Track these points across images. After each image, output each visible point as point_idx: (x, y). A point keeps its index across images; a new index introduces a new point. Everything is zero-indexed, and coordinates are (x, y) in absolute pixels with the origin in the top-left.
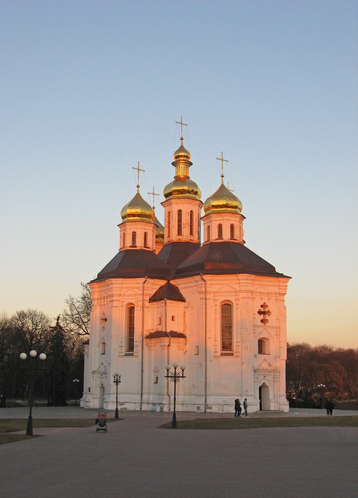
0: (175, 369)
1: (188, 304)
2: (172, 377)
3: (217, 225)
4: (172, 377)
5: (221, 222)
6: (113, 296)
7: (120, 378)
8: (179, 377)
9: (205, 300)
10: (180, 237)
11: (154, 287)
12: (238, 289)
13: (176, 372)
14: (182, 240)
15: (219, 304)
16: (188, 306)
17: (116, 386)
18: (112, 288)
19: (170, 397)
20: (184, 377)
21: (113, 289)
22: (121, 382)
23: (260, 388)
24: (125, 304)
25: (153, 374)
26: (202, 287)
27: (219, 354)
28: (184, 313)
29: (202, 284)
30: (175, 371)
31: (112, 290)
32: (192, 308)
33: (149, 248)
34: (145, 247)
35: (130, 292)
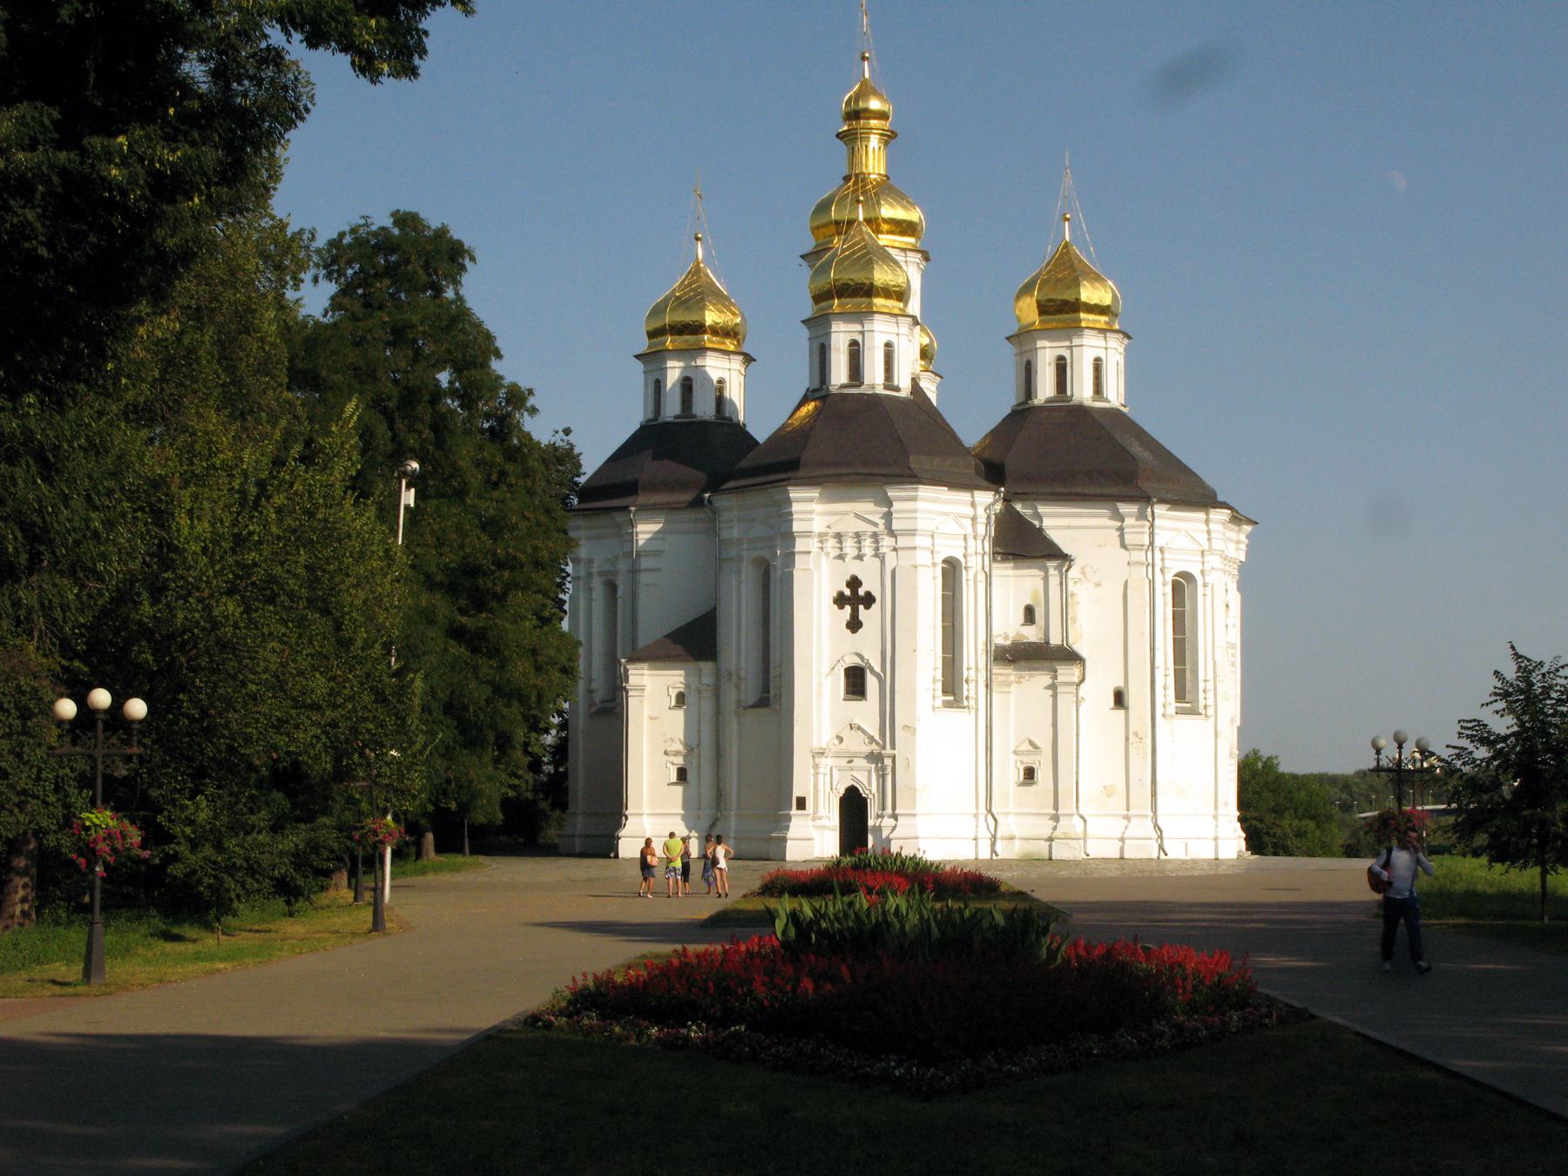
1: (1083, 573)
3: (1091, 361)
5: (1102, 354)
6: (914, 535)
9: (1145, 568)
12: (1206, 546)
15: (1169, 577)
16: (1082, 576)
18: (915, 511)
19: (1085, 821)
21: (918, 515)
24: (939, 559)
25: (1013, 757)
26: (1143, 533)
27: (1171, 710)
29: (1143, 526)
31: (916, 518)
32: (1098, 585)
35: (950, 526)
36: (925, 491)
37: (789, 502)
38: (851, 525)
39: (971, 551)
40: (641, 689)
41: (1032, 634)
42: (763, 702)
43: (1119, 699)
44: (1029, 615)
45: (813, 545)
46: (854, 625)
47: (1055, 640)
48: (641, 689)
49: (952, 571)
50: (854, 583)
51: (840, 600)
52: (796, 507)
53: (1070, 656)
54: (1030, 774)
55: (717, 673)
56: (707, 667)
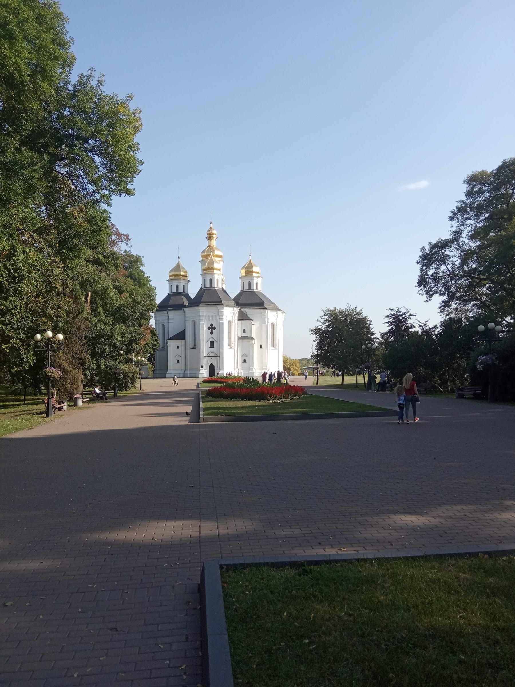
15: (270, 324)
36: (225, 308)
37: (199, 309)
38: (210, 314)
39: (233, 319)
40: (170, 345)
41: (244, 334)
42: (194, 348)
43: (261, 347)
44: (244, 331)
45: (204, 318)
46: (212, 333)
48: (170, 345)
49: (230, 322)
50: (212, 325)
51: (209, 328)
52: (200, 311)
53: (253, 339)
54: (245, 361)
55: (185, 342)
56: (183, 341)
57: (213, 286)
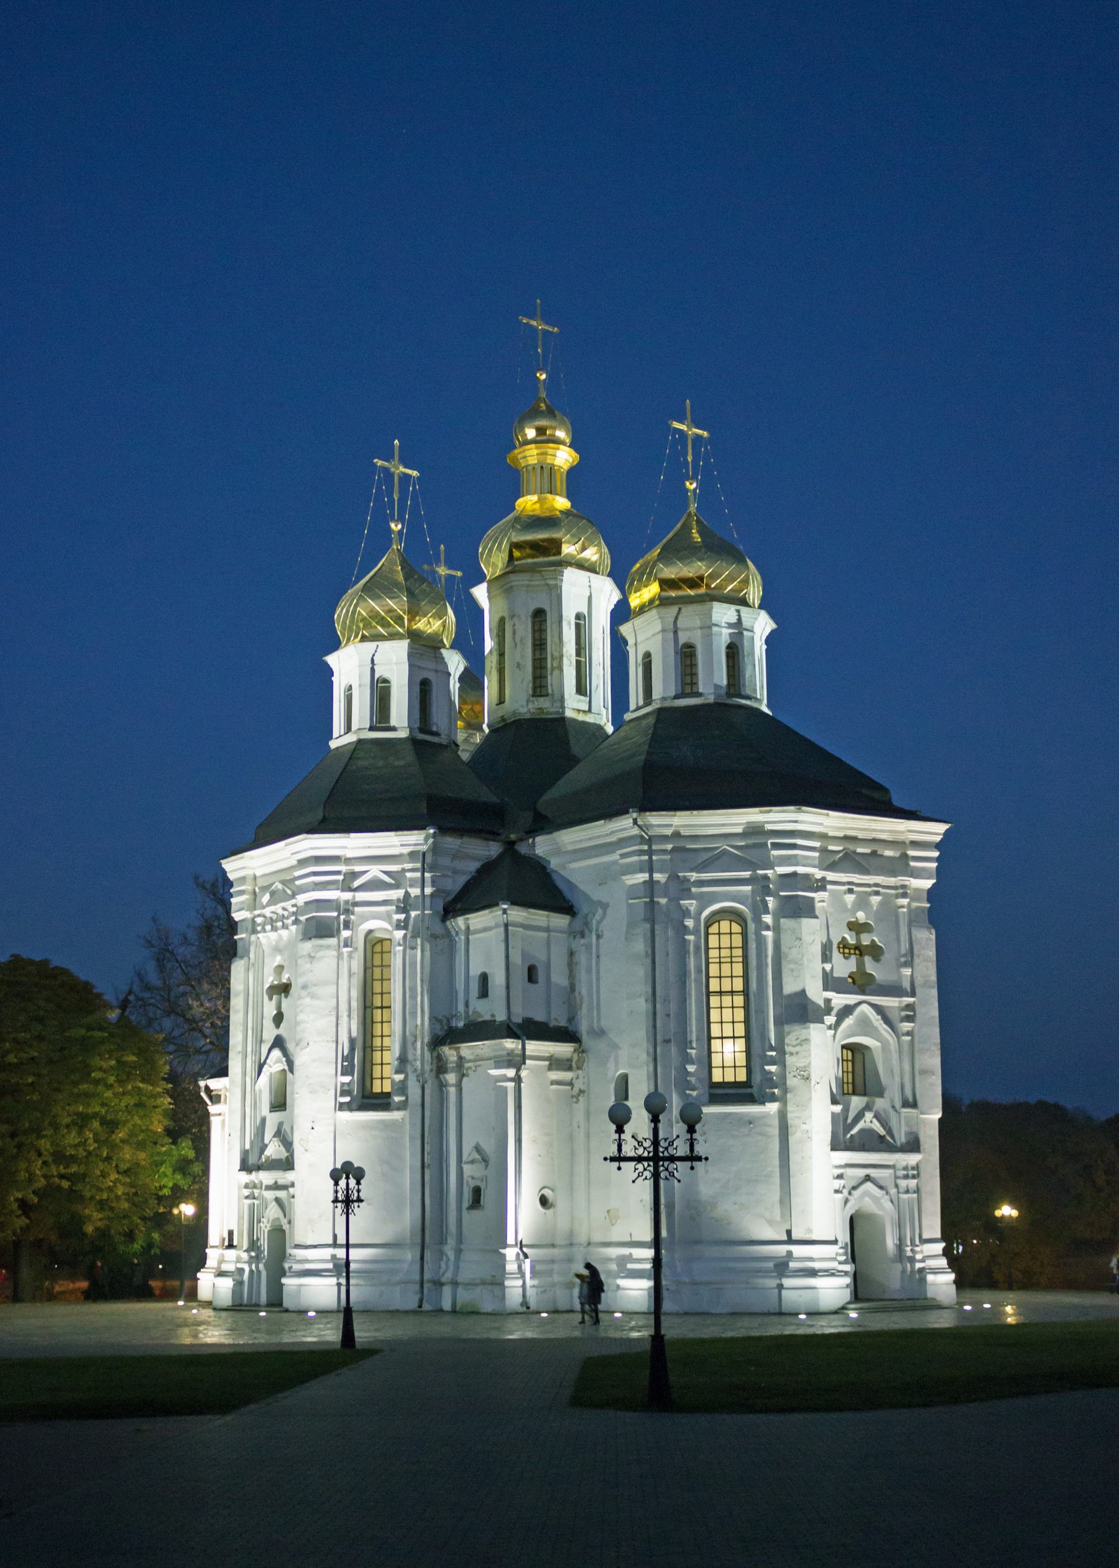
0: (655, 1120)
2: (639, 1159)
4: (639, 1159)
7: (358, 1183)
8: (673, 1159)
10: (544, 703)
11: (460, 865)
13: (661, 1135)
14: (548, 713)
17: (344, 1216)
20: (699, 1159)
22: (362, 1201)
23: (852, 1219)
28: (571, 954)
30: (656, 1131)
33: (437, 734)
34: (422, 730)
46: (278, 1019)
47: (501, 1017)
57: (355, 726)
